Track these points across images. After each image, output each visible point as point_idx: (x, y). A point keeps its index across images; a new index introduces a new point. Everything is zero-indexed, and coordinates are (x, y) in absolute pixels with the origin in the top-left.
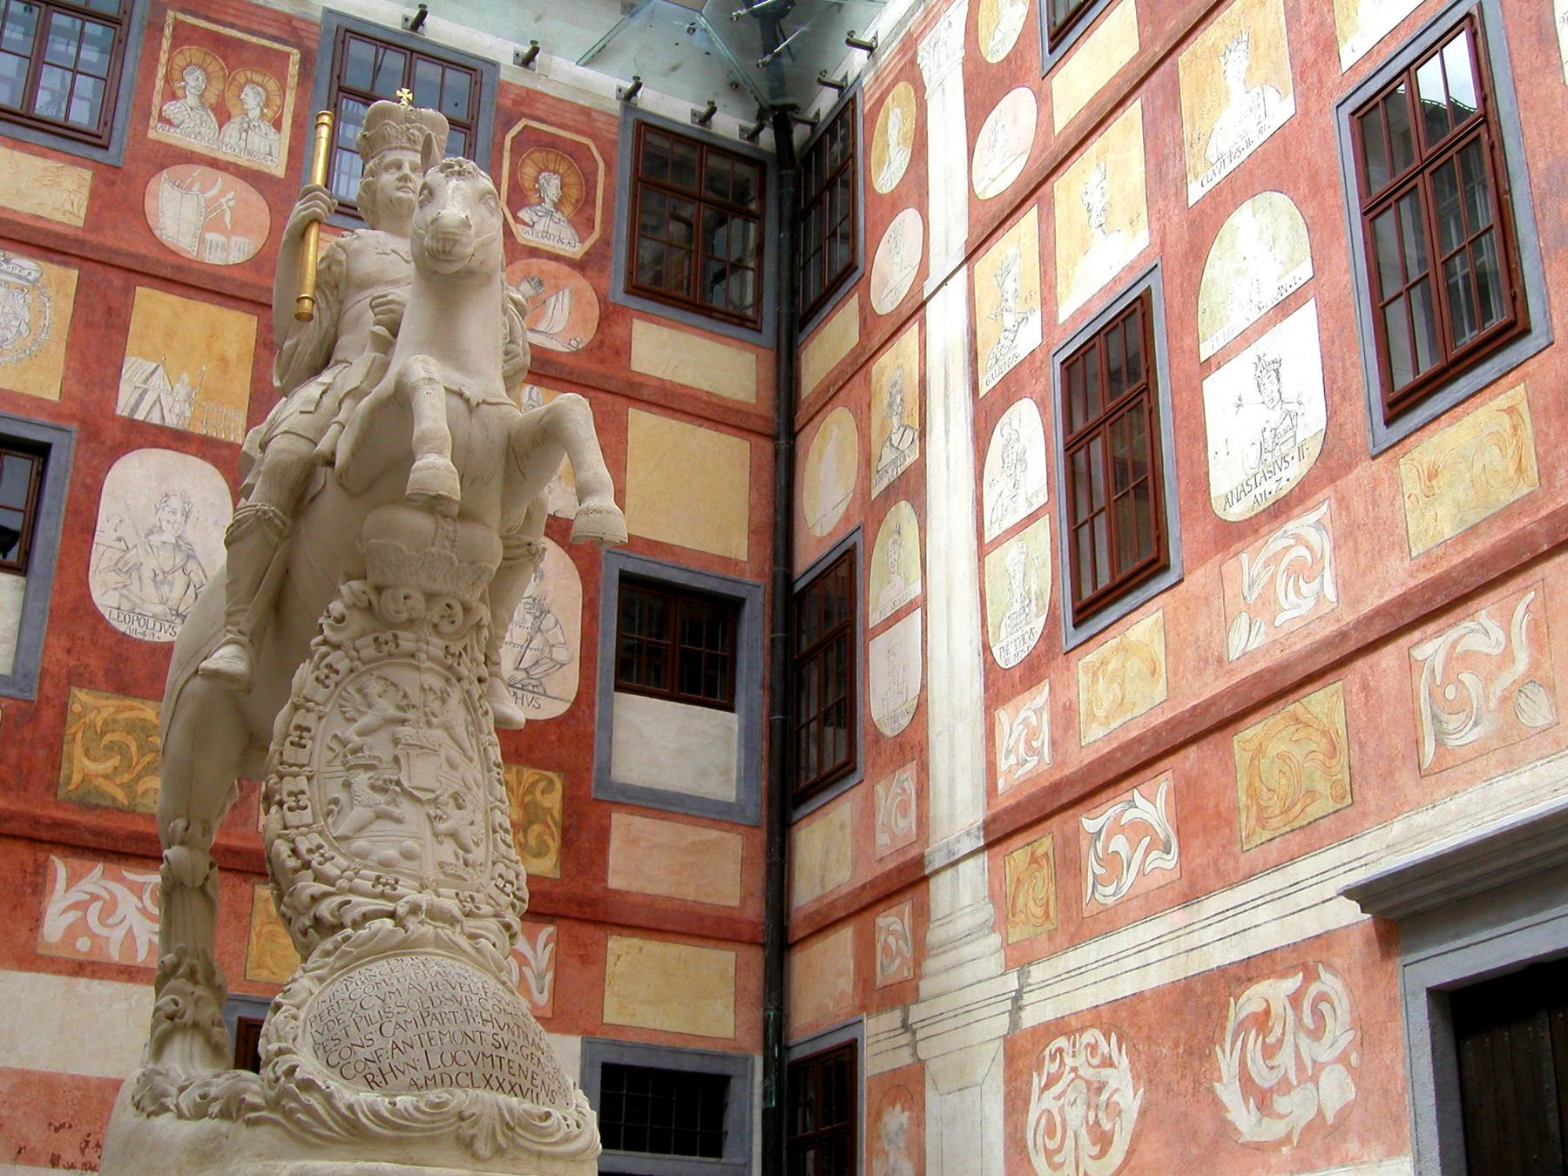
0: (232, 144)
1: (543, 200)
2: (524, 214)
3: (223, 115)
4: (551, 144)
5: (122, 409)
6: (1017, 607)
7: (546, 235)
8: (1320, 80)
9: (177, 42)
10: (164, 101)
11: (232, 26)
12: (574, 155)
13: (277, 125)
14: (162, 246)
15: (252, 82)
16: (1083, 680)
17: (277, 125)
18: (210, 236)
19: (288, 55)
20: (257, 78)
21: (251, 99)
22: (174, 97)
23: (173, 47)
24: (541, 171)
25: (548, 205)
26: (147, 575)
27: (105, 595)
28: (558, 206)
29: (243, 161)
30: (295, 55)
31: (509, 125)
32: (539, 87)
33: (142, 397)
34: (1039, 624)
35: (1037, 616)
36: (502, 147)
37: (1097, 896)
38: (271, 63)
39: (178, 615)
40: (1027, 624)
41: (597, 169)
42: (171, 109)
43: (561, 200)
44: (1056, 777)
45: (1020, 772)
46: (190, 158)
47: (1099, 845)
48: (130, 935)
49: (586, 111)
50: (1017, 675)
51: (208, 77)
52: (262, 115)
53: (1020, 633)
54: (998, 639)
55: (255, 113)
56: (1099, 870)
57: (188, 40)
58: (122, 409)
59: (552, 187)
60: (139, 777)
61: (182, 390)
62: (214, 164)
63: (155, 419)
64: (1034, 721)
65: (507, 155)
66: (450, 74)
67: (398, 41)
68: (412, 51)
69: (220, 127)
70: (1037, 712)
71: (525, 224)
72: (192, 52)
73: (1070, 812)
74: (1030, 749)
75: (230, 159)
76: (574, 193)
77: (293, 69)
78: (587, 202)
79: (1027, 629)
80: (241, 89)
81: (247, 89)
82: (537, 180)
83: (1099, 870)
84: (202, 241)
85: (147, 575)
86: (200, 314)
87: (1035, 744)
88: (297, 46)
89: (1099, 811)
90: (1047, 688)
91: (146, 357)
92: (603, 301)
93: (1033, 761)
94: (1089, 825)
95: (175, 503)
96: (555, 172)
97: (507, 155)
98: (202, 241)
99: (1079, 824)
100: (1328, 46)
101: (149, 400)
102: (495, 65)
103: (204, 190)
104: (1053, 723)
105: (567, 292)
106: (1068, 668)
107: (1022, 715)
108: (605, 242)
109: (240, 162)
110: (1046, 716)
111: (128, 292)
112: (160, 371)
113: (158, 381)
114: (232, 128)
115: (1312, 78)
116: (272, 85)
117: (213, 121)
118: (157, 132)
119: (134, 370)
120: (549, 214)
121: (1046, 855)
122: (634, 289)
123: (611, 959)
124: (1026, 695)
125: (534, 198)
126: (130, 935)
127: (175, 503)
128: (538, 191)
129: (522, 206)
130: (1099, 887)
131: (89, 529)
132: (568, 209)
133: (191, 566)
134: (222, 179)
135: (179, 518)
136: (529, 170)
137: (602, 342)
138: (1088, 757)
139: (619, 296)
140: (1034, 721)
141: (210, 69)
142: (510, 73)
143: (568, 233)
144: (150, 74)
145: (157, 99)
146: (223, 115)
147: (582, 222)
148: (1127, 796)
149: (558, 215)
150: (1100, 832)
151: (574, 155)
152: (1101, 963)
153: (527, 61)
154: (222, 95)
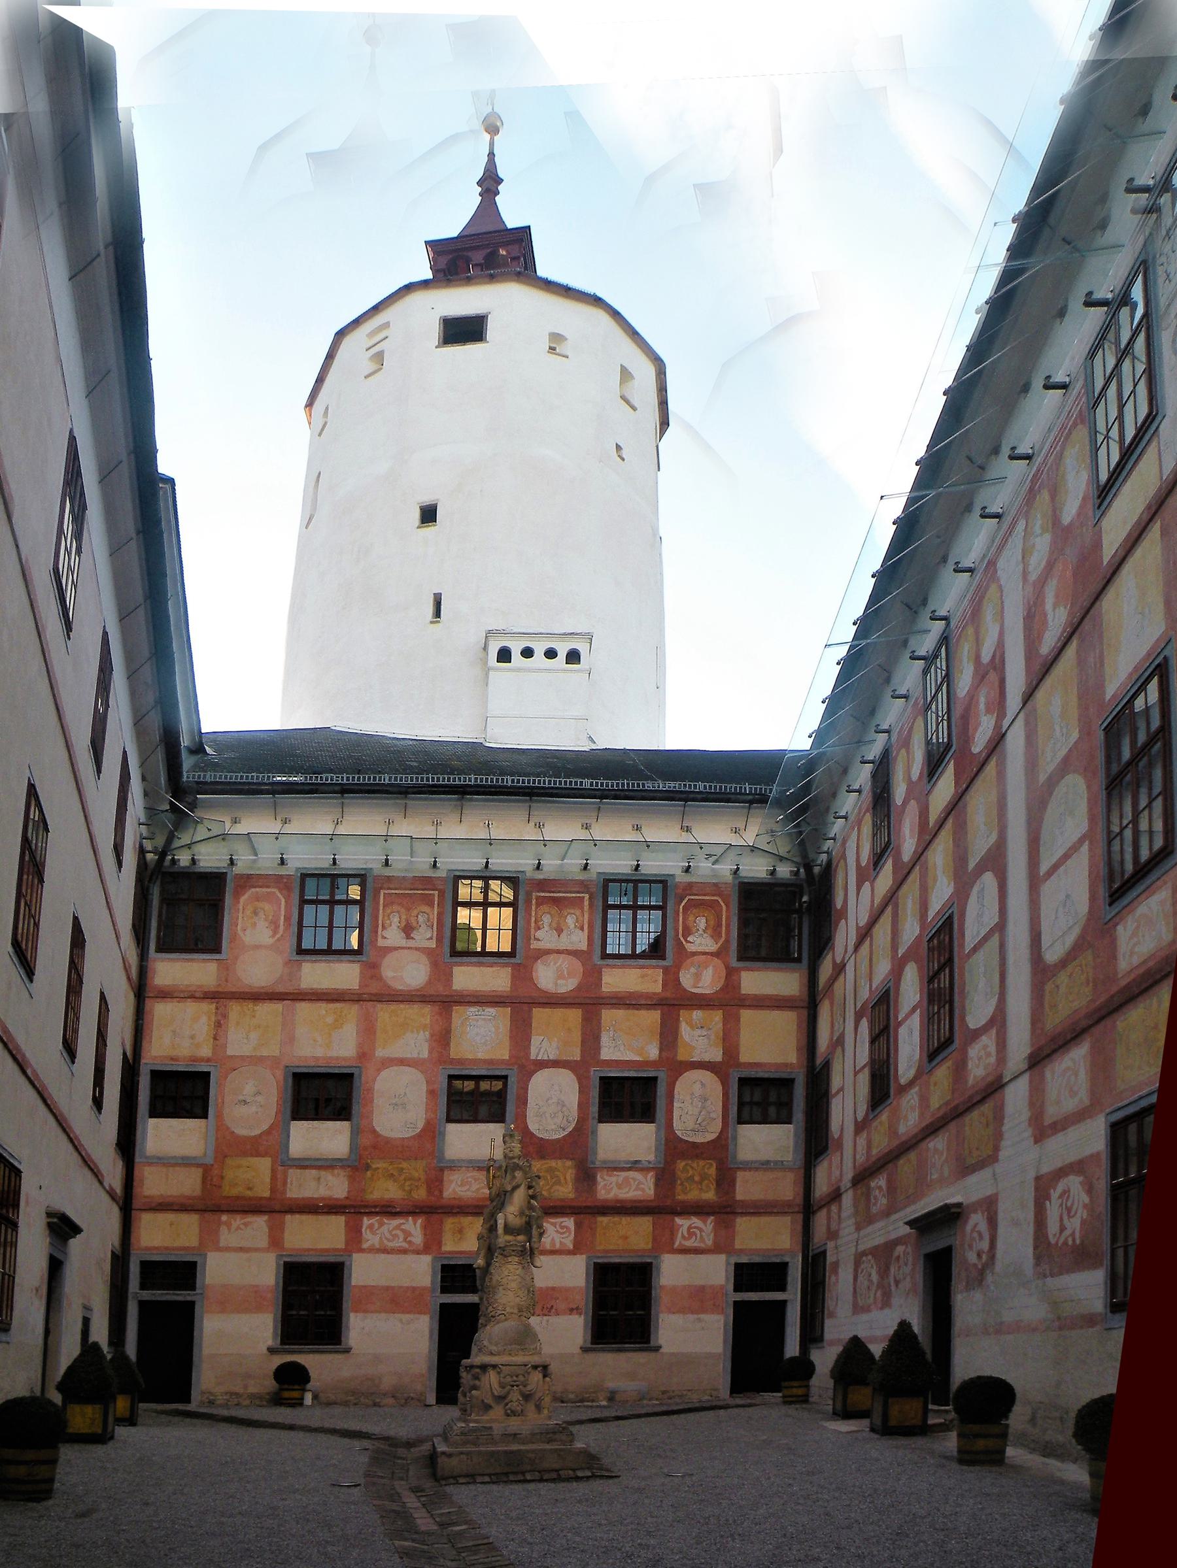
0: (564, 942)
3: (559, 931)
4: (701, 904)
5: (533, 1057)
9: (538, 905)
10: (536, 931)
11: (559, 892)
12: (712, 905)
13: (582, 929)
14: (540, 990)
21: (570, 921)
22: (539, 929)
23: (537, 908)
25: (701, 932)
26: (548, 1115)
27: (533, 1126)
30: (587, 896)
33: (539, 1050)
39: (561, 1128)
41: (722, 910)
42: (539, 934)
46: (548, 952)
48: (553, 1239)
49: (715, 885)
52: (576, 926)
57: (542, 904)
58: (533, 1057)
59: (702, 922)
60: (552, 1186)
61: (554, 1045)
62: (559, 952)
63: (546, 1058)
65: (681, 914)
68: (636, 880)
72: (545, 908)
76: (712, 923)
77: (586, 903)
78: (719, 925)
84: (556, 984)
85: (548, 1115)
86: (558, 1013)
91: (540, 1035)
92: (727, 967)
95: (556, 1087)
97: (681, 914)
101: (541, 1053)
102: (672, 875)
103: (555, 964)
105: (711, 968)
108: (727, 941)
111: (530, 1011)
112: (546, 1039)
113: (545, 1043)
114: (564, 935)
116: (578, 912)
118: (534, 945)
119: (535, 1041)
122: (741, 958)
123: (738, 1225)
125: (694, 930)
126: (553, 1239)
127: (556, 1087)
131: (525, 1102)
132: (710, 931)
133: (564, 1109)
135: (559, 1092)
136: (691, 918)
137: (728, 985)
139: (734, 963)
141: (552, 913)
142: (681, 878)
144: (529, 922)
145: (533, 931)
146: (559, 931)
147: (715, 932)
149: (705, 935)
151: (712, 905)
153: (687, 870)
154: (558, 923)
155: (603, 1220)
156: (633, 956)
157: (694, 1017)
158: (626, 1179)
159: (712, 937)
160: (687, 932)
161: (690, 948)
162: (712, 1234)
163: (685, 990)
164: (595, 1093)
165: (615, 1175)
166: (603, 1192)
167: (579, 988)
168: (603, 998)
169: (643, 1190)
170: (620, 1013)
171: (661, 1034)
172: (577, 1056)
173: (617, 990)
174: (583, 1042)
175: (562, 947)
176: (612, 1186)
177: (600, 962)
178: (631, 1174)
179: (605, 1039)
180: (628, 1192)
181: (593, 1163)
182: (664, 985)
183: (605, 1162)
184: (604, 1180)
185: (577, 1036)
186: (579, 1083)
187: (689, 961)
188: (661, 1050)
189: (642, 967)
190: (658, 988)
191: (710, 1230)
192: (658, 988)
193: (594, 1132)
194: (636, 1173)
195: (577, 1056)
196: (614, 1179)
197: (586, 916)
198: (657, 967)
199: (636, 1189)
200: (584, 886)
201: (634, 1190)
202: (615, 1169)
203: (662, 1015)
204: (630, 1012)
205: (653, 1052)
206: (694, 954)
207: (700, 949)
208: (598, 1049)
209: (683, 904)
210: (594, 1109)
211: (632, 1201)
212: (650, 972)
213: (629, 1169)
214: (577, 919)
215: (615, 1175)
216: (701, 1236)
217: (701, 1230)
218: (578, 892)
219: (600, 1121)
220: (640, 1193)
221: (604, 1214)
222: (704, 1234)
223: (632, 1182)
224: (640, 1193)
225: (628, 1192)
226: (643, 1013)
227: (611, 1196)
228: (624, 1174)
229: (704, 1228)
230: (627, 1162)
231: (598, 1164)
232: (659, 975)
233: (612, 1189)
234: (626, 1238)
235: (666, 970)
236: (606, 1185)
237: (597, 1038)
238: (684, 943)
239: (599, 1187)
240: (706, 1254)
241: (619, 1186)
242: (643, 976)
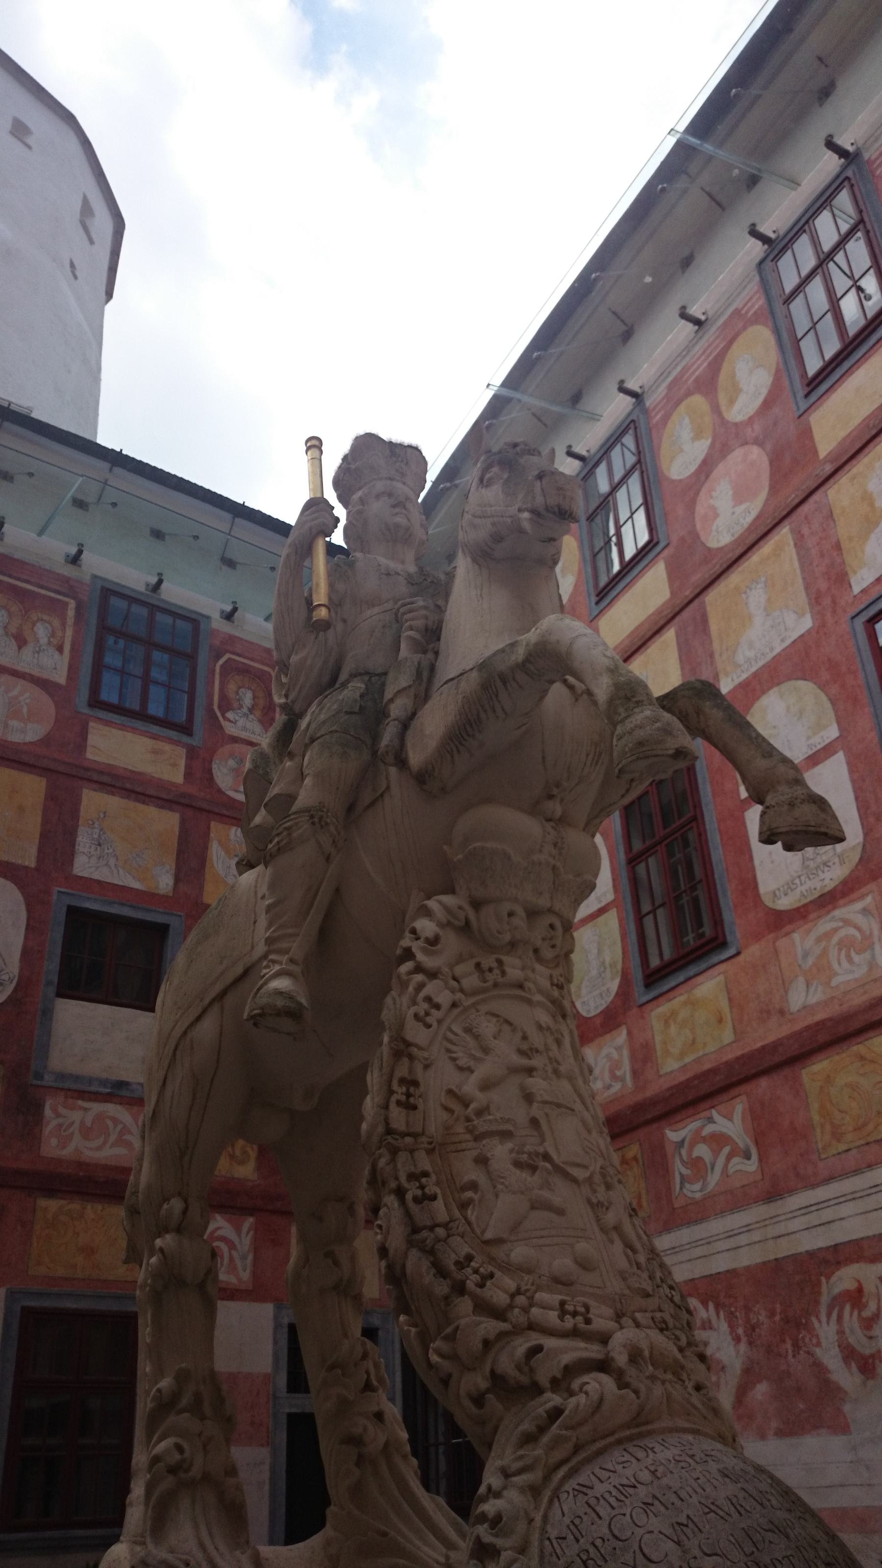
1: (241, 707)
2: (230, 715)
3: (21, 642)
4: (245, 671)
6: (594, 973)
7: (244, 729)
8: (834, 602)
13: (60, 649)
15: (42, 620)
16: (657, 1026)
17: (60, 649)
18: (14, 723)
19: (66, 604)
20: (45, 617)
21: (42, 631)
24: (240, 688)
25: (245, 710)
28: (251, 710)
29: (36, 672)
30: (72, 604)
31: (218, 657)
32: (237, 634)
34: (614, 985)
35: (613, 979)
36: (214, 671)
37: (685, 1191)
38: (56, 608)
40: (604, 985)
43: (253, 706)
44: (640, 1097)
45: (606, 1094)
47: (684, 1152)
50: (598, 1021)
51: (10, 615)
52: (49, 643)
53: (598, 992)
54: (579, 996)
55: (44, 640)
56: (685, 1171)
59: (248, 699)
62: (15, 673)
64: (615, 1055)
65: (217, 677)
66: (179, 622)
67: (142, 598)
68: (153, 606)
69: (20, 648)
70: (619, 1049)
71: (229, 720)
73: (655, 1126)
74: (614, 1077)
75: (27, 671)
76: (261, 702)
77: (71, 613)
79: (604, 988)
80: (34, 624)
81: (39, 625)
82: (237, 693)
83: (685, 1171)
87: (618, 1073)
88: (74, 598)
89: (680, 1125)
90: (624, 1032)
93: (617, 1087)
94: (673, 1135)
96: (249, 688)
97: (217, 677)
98: (6, 726)
99: (663, 1135)
100: (841, 578)
102: (208, 618)
104: (633, 1057)
106: (643, 1018)
107: (605, 1051)
109: (33, 673)
110: (626, 1053)
114: (27, 652)
115: (827, 601)
116: (56, 623)
117: (14, 645)
120: (245, 715)
121: (635, 1159)
124: (607, 1037)
125: (236, 705)
128: (239, 700)
129: (228, 710)
130: (687, 1185)
132: (258, 713)
134: (22, 682)
136: (232, 687)
138: (665, 1084)
140: (615, 1055)
142: (218, 624)
143: (258, 728)
146: (21, 642)
148: (706, 1114)
149: (251, 717)
150: (683, 1141)
152: (694, 1245)
153: (229, 617)
155: (51, 1205)
156: (142, 715)
157: (232, 837)
158: (100, 1118)
159: (261, 721)
160: (226, 705)
161: (230, 729)
162: (250, 1257)
163: (220, 791)
164: (57, 934)
165: (81, 1108)
166: (54, 1142)
167: (46, 741)
168: (87, 769)
169: (129, 1144)
170: (114, 803)
171: (180, 853)
172: (30, 860)
173: (111, 762)
174: (44, 835)
175: (21, 667)
176: (71, 1130)
177: (86, 711)
178: (112, 1109)
179: (84, 840)
180: (99, 1148)
181: (39, 1076)
182: (188, 774)
183: (61, 1076)
184: (58, 1115)
185: (33, 824)
186: (29, 911)
187: (228, 748)
188: (177, 880)
189: (154, 737)
190: (178, 777)
191: (246, 1248)
192: (178, 777)
193: (48, 1013)
194: (119, 1107)
195: (30, 860)
196: (76, 1116)
197: (69, 633)
198: (177, 743)
199: (120, 1142)
200: (70, 587)
201: (113, 1145)
202: (82, 1094)
203: (183, 822)
204: (132, 804)
205: (165, 882)
206: (235, 740)
207: (244, 735)
208: (70, 854)
209: (221, 662)
210: (51, 967)
211: (106, 1167)
212: (167, 747)
213: (107, 1098)
214: (53, 631)
215: (81, 1108)
216: (231, 1259)
217: (231, 1245)
218: (59, 593)
219: (60, 995)
220: (121, 1151)
221: (51, 1192)
222: (234, 1253)
223: (110, 1123)
224: (121, 1151)
225: (99, 1148)
226: (152, 811)
227: (67, 1152)
228: (96, 1108)
229: (236, 1240)
230: (104, 1082)
231: (48, 1080)
232: (180, 756)
233: (70, 1137)
234: (89, 1251)
235: (192, 753)
236: (60, 1126)
237: (71, 835)
238: (221, 719)
239: (47, 1130)
240: (240, 1299)
241: (86, 1132)
242: (155, 752)
